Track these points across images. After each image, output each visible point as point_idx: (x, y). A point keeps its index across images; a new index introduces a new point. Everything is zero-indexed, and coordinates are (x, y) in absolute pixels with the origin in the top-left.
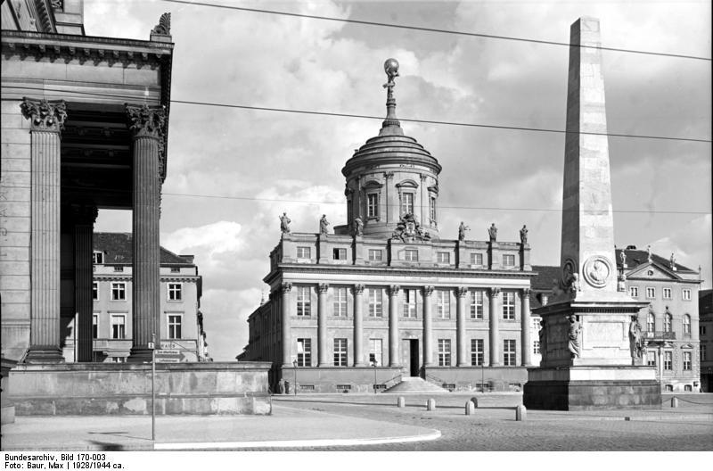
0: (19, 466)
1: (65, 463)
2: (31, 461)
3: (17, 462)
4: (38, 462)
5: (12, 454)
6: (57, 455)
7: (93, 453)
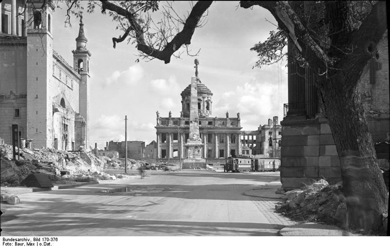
0: (10, 244)
1: (35, 242)
3: (9, 242)
4: (21, 242)
5: (6, 238)
6: (31, 238)
7: (52, 237)
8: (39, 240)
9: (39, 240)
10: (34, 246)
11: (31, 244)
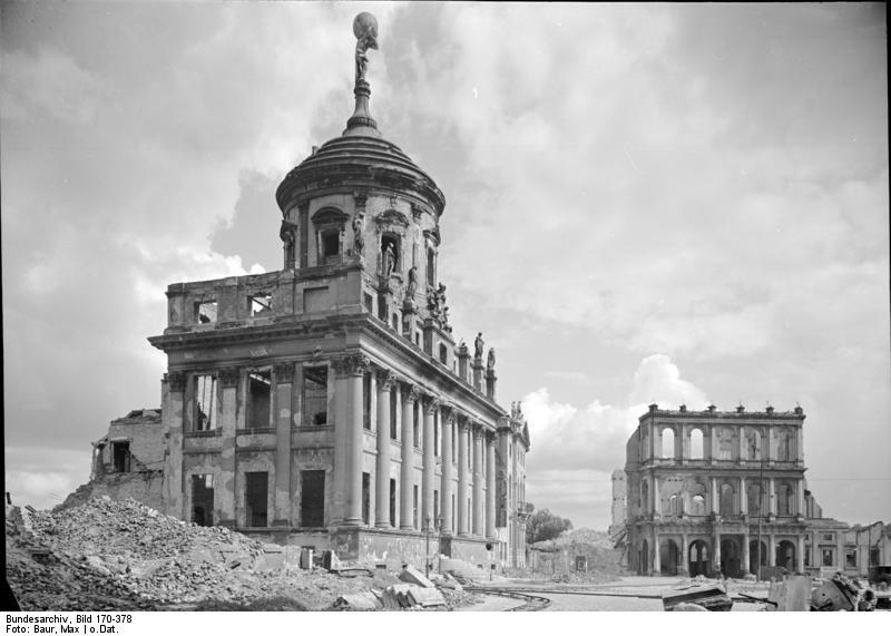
0: (24, 630)
1: (81, 626)
2: (39, 624)
3: (21, 625)
4: (47, 625)
6: (72, 616)
8: (90, 620)
9: (90, 620)
11: (70, 630)
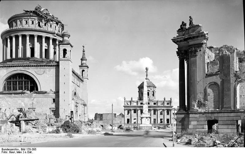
0: (6, 152)
1: (22, 151)
2: (11, 151)
3: (6, 151)
4: (13, 151)
5: (4, 148)
6: (20, 148)
9: (25, 149)
10: (21, 153)
11: (19, 152)
